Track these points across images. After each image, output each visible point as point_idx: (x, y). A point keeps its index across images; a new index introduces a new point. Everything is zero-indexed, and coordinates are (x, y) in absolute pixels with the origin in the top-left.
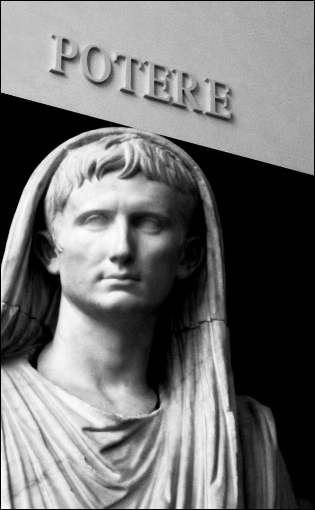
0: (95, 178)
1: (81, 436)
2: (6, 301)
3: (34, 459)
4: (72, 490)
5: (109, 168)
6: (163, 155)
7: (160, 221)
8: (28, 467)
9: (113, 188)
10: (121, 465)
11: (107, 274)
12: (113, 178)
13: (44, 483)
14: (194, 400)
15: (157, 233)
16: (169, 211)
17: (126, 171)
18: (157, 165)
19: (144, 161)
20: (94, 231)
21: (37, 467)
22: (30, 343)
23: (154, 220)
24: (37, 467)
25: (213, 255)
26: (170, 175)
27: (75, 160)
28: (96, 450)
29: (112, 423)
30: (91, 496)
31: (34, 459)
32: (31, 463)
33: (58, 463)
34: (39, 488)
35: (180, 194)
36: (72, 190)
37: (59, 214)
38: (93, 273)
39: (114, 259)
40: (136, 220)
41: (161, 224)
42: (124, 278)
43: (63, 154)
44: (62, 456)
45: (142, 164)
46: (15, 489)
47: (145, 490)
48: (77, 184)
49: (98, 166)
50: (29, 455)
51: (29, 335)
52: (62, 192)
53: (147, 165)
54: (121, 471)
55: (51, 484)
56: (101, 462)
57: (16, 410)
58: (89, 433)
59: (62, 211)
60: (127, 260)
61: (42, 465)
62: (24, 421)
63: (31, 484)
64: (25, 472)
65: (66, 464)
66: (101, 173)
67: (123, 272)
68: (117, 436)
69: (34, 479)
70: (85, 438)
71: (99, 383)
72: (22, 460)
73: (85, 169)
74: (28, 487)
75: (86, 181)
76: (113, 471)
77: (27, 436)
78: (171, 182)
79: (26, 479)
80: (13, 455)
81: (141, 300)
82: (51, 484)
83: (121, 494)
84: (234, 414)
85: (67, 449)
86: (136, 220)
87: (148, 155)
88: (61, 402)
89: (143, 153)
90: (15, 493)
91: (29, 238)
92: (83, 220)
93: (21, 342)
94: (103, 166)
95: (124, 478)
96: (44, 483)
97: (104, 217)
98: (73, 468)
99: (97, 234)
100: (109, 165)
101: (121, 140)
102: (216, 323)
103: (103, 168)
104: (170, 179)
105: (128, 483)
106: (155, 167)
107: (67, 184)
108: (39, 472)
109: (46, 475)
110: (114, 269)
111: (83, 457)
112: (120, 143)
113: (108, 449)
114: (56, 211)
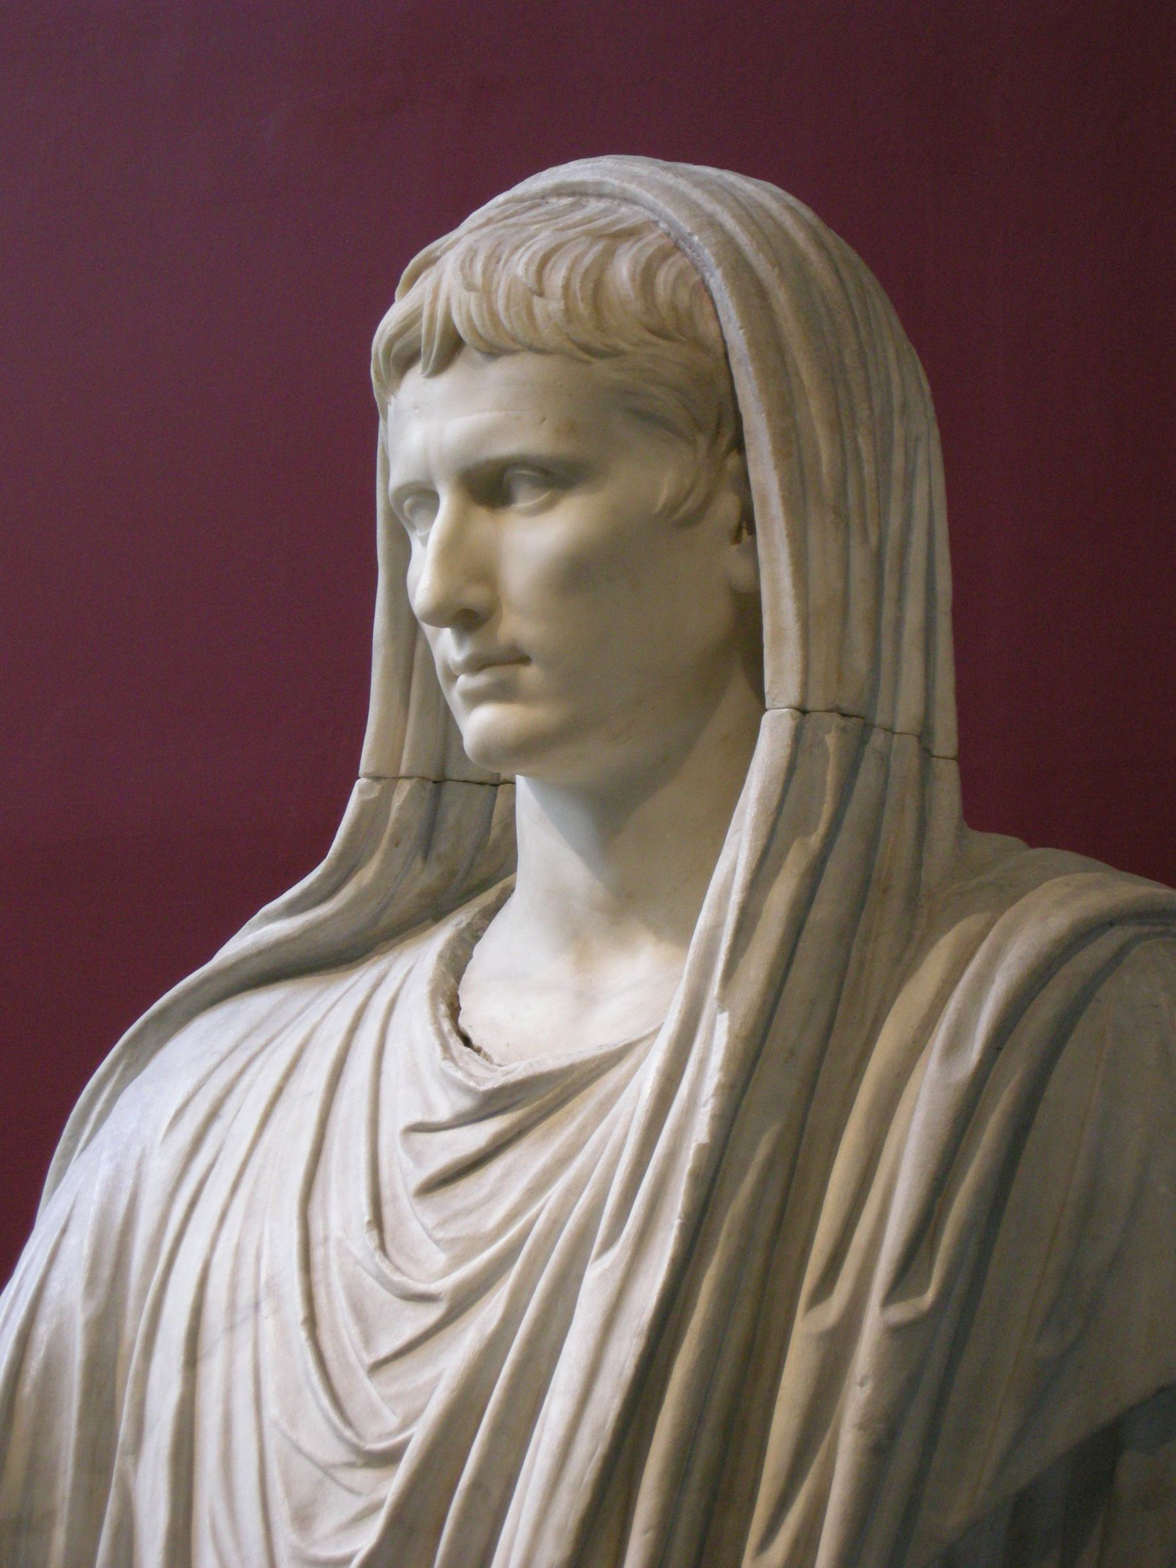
2: (371, 770)
4: (311, 1322)
6: (528, 264)
9: (417, 411)
13: (266, 1308)
16: (570, 428)
29: (466, 1103)
35: (599, 365)
42: (476, 665)
53: (470, 318)
55: (276, 1311)
64: (233, 1287)
74: (231, 1328)
79: (232, 1306)
83: (431, 1314)
84: (732, 1018)
87: (470, 287)
95: (458, 1261)
101: (438, 253)
105: (444, 1285)
106: (493, 314)
112: (437, 259)
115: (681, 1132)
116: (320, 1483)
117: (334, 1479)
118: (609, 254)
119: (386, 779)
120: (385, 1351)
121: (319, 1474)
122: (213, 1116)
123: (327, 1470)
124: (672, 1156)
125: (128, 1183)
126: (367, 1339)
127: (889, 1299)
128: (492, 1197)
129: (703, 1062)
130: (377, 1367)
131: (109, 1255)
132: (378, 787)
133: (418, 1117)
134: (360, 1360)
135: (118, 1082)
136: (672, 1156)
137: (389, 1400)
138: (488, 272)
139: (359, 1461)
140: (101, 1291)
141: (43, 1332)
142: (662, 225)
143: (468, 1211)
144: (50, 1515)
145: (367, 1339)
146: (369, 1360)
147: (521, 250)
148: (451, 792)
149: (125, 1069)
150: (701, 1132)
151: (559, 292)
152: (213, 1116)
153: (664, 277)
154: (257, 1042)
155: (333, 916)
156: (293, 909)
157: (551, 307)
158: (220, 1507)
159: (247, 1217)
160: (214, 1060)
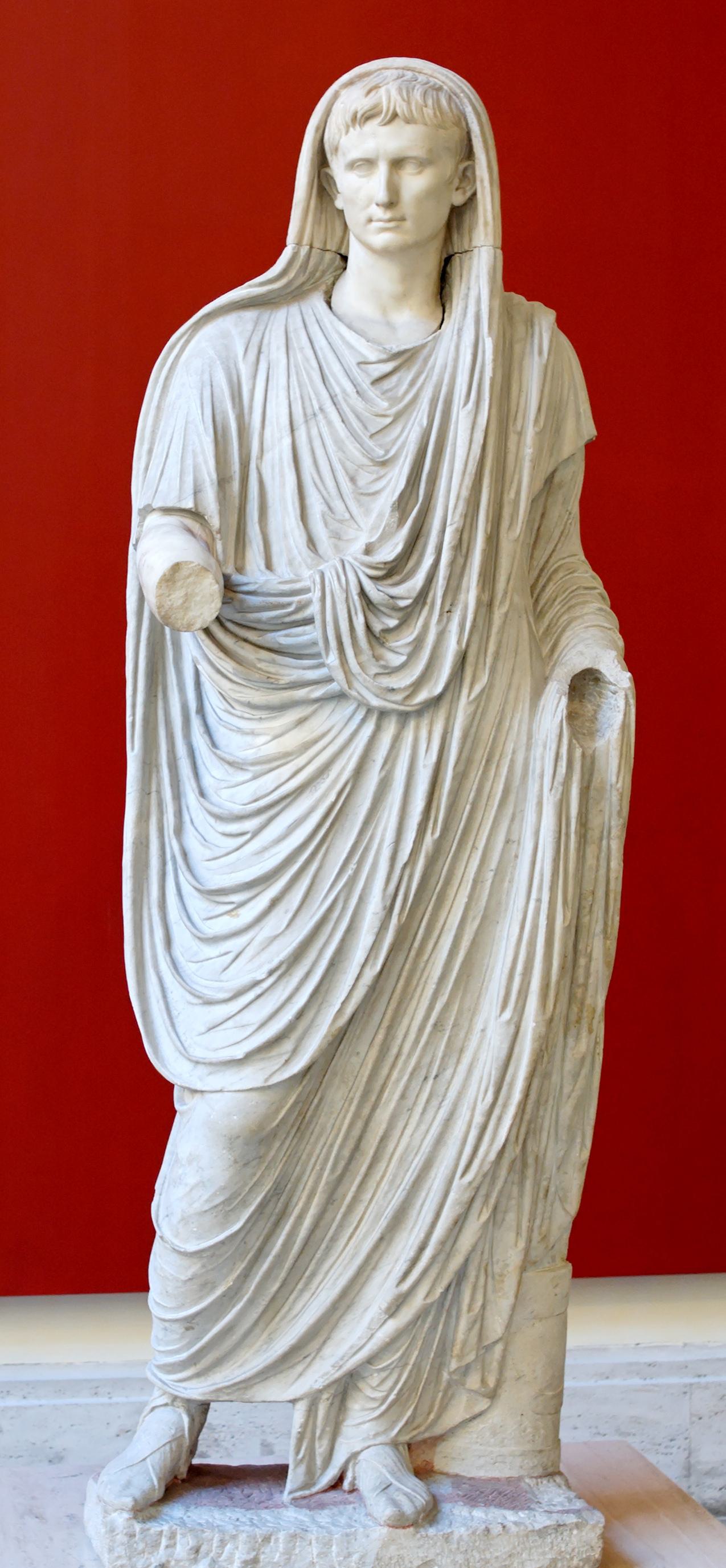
0: (357, 127)
1: (356, 371)
3: (313, 396)
4: (343, 421)
5: (368, 116)
7: (421, 162)
8: (307, 403)
10: (389, 394)
11: (374, 219)
12: (373, 125)
13: (320, 417)
14: (463, 326)
15: (420, 173)
16: (430, 151)
17: (383, 120)
18: (413, 108)
19: (400, 107)
20: (360, 177)
21: (315, 402)
22: (328, 273)
23: (414, 161)
24: (315, 402)
25: (482, 181)
26: (428, 115)
27: (342, 105)
28: (368, 382)
29: (384, 356)
30: (360, 425)
31: (313, 396)
32: (310, 400)
33: (333, 398)
34: (316, 421)
36: (341, 137)
37: (334, 157)
38: (363, 217)
39: (378, 205)
40: (397, 164)
41: (422, 164)
42: (390, 220)
43: (336, 96)
44: (338, 390)
45: (398, 111)
46: (295, 424)
47: (411, 414)
48: (344, 132)
49: (359, 116)
50: (309, 393)
51: (325, 266)
52: (333, 139)
53: (403, 111)
54: (389, 399)
55: (326, 417)
56: (372, 393)
57: (302, 349)
58: (363, 366)
59: (336, 155)
60: (392, 203)
61: (318, 400)
62: (307, 360)
63: (308, 418)
64: (304, 408)
65: (340, 397)
66: (362, 121)
67: (388, 215)
68: (388, 367)
69: (312, 413)
70: (358, 370)
71: (384, 311)
72: (302, 398)
73: (348, 118)
74: (306, 421)
75: (351, 129)
76: (383, 400)
77: (308, 374)
78: (429, 123)
79: (305, 415)
80: (295, 393)
81: (409, 238)
82: (326, 417)
83: (388, 420)
84: (492, 339)
85: (341, 383)
86: (397, 164)
88: (342, 337)
89: (399, 98)
90: (295, 428)
91: (314, 177)
92: (352, 165)
93: (318, 274)
94: (362, 116)
95: (391, 406)
96: (320, 417)
97: (369, 163)
98: (345, 400)
99: (364, 180)
100: (368, 113)
101: (381, 85)
102: (484, 249)
103: (363, 118)
104: (427, 119)
106: (411, 111)
107: (336, 131)
108: (316, 407)
109: (321, 409)
110: (379, 213)
111: (355, 390)
112: (380, 87)
113: (377, 381)
114: (332, 154)
115: (482, 373)
116: (356, 470)
117: (362, 469)
118: (437, 95)
119: (299, 244)
120: (373, 431)
121: (356, 467)
122: (259, 352)
123: (361, 466)
124: (481, 379)
125: (234, 372)
126: (366, 428)
127: (534, 426)
128: (397, 386)
129: (484, 352)
130: (372, 436)
131: (236, 394)
132: (297, 246)
133: (362, 360)
134: (364, 434)
135: (190, 335)
136: (481, 379)
137: (381, 446)
138: (408, 97)
139: (371, 464)
140: (237, 406)
141: (218, 418)
142: (445, 87)
143: (390, 390)
144: (231, 477)
145: (366, 428)
146: (369, 434)
147: (415, 91)
148: (314, 250)
149: (193, 331)
150: (488, 373)
151: (431, 107)
152: (259, 352)
153: (453, 106)
154: (261, 328)
155: (279, 289)
156: (262, 284)
157: (429, 111)
158: (316, 476)
159: (300, 386)
160: (249, 333)
